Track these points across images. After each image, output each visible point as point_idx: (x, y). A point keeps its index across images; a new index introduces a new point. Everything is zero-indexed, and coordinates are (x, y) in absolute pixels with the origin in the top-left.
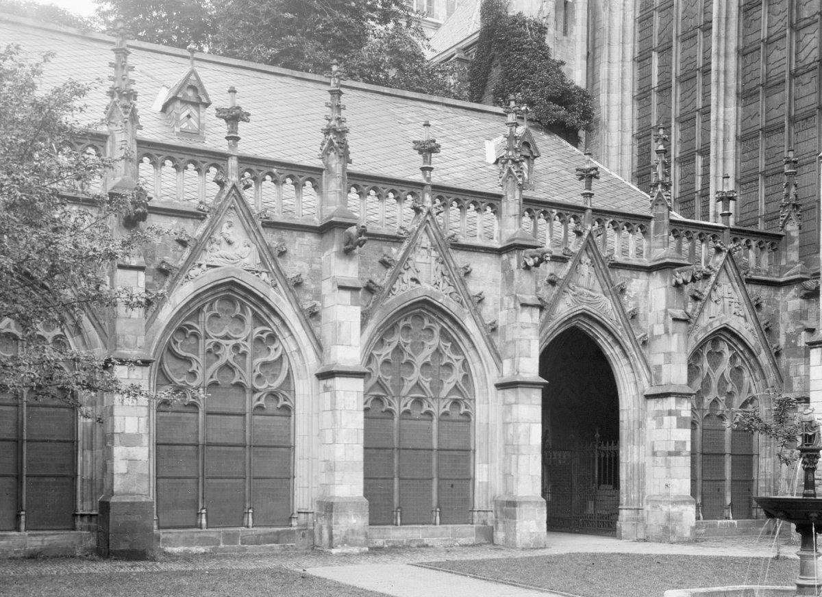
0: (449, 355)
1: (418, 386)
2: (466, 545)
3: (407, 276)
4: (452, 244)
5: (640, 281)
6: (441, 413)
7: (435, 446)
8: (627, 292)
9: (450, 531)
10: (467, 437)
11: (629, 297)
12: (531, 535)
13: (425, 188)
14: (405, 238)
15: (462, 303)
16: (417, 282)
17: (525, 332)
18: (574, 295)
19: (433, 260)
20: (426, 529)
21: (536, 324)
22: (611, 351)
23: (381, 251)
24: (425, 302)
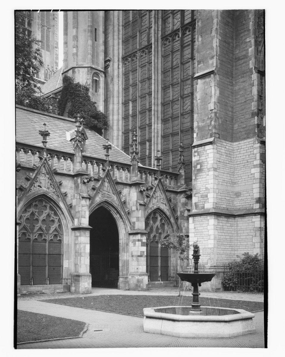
0: (53, 217)
1: (40, 229)
2: (59, 293)
3: (37, 184)
5: (127, 189)
6: (50, 239)
7: (47, 253)
8: (122, 194)
9: (53, 287)
11: (123, 195)
12: (85, 288)
14: (36, 169)
16: (41, 187)
17: (84, 208)
18: (102, 194)
19: (47, 178)
20: (44, 286)
22: (116, 216)
24: (44, 195)
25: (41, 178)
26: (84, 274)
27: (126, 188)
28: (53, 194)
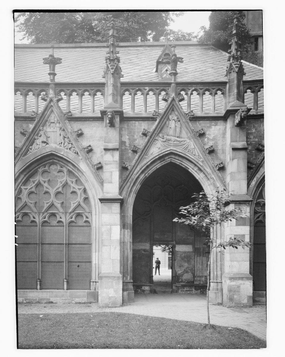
0: (74, 186)
1: (52, 205)
2: (80, 303)
3: (39, 141)
4: (67, 118)
5: (218, 127)
7: (65, 243)
8: (207, 136)
10: (90, 235)
11: (208, 139)
12: (110, 298)
13: (50, 86)
14: (35, 118)
15: (77, 153)
16: (47, 144)
18: (163, 142)
19: (58, 129)
20: (52, 292)
21: (116, 161)
22: (199, 176)
23: (22, 126)
24: (52, 155)
25: (48, 130)
26: (107, 275)
27: (216, 125)
28: (67, 152)
